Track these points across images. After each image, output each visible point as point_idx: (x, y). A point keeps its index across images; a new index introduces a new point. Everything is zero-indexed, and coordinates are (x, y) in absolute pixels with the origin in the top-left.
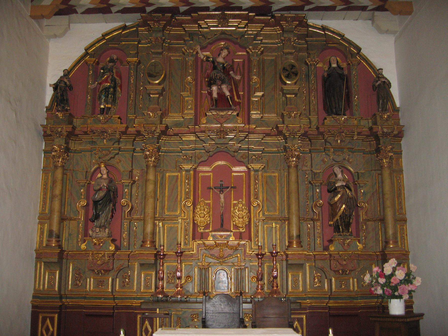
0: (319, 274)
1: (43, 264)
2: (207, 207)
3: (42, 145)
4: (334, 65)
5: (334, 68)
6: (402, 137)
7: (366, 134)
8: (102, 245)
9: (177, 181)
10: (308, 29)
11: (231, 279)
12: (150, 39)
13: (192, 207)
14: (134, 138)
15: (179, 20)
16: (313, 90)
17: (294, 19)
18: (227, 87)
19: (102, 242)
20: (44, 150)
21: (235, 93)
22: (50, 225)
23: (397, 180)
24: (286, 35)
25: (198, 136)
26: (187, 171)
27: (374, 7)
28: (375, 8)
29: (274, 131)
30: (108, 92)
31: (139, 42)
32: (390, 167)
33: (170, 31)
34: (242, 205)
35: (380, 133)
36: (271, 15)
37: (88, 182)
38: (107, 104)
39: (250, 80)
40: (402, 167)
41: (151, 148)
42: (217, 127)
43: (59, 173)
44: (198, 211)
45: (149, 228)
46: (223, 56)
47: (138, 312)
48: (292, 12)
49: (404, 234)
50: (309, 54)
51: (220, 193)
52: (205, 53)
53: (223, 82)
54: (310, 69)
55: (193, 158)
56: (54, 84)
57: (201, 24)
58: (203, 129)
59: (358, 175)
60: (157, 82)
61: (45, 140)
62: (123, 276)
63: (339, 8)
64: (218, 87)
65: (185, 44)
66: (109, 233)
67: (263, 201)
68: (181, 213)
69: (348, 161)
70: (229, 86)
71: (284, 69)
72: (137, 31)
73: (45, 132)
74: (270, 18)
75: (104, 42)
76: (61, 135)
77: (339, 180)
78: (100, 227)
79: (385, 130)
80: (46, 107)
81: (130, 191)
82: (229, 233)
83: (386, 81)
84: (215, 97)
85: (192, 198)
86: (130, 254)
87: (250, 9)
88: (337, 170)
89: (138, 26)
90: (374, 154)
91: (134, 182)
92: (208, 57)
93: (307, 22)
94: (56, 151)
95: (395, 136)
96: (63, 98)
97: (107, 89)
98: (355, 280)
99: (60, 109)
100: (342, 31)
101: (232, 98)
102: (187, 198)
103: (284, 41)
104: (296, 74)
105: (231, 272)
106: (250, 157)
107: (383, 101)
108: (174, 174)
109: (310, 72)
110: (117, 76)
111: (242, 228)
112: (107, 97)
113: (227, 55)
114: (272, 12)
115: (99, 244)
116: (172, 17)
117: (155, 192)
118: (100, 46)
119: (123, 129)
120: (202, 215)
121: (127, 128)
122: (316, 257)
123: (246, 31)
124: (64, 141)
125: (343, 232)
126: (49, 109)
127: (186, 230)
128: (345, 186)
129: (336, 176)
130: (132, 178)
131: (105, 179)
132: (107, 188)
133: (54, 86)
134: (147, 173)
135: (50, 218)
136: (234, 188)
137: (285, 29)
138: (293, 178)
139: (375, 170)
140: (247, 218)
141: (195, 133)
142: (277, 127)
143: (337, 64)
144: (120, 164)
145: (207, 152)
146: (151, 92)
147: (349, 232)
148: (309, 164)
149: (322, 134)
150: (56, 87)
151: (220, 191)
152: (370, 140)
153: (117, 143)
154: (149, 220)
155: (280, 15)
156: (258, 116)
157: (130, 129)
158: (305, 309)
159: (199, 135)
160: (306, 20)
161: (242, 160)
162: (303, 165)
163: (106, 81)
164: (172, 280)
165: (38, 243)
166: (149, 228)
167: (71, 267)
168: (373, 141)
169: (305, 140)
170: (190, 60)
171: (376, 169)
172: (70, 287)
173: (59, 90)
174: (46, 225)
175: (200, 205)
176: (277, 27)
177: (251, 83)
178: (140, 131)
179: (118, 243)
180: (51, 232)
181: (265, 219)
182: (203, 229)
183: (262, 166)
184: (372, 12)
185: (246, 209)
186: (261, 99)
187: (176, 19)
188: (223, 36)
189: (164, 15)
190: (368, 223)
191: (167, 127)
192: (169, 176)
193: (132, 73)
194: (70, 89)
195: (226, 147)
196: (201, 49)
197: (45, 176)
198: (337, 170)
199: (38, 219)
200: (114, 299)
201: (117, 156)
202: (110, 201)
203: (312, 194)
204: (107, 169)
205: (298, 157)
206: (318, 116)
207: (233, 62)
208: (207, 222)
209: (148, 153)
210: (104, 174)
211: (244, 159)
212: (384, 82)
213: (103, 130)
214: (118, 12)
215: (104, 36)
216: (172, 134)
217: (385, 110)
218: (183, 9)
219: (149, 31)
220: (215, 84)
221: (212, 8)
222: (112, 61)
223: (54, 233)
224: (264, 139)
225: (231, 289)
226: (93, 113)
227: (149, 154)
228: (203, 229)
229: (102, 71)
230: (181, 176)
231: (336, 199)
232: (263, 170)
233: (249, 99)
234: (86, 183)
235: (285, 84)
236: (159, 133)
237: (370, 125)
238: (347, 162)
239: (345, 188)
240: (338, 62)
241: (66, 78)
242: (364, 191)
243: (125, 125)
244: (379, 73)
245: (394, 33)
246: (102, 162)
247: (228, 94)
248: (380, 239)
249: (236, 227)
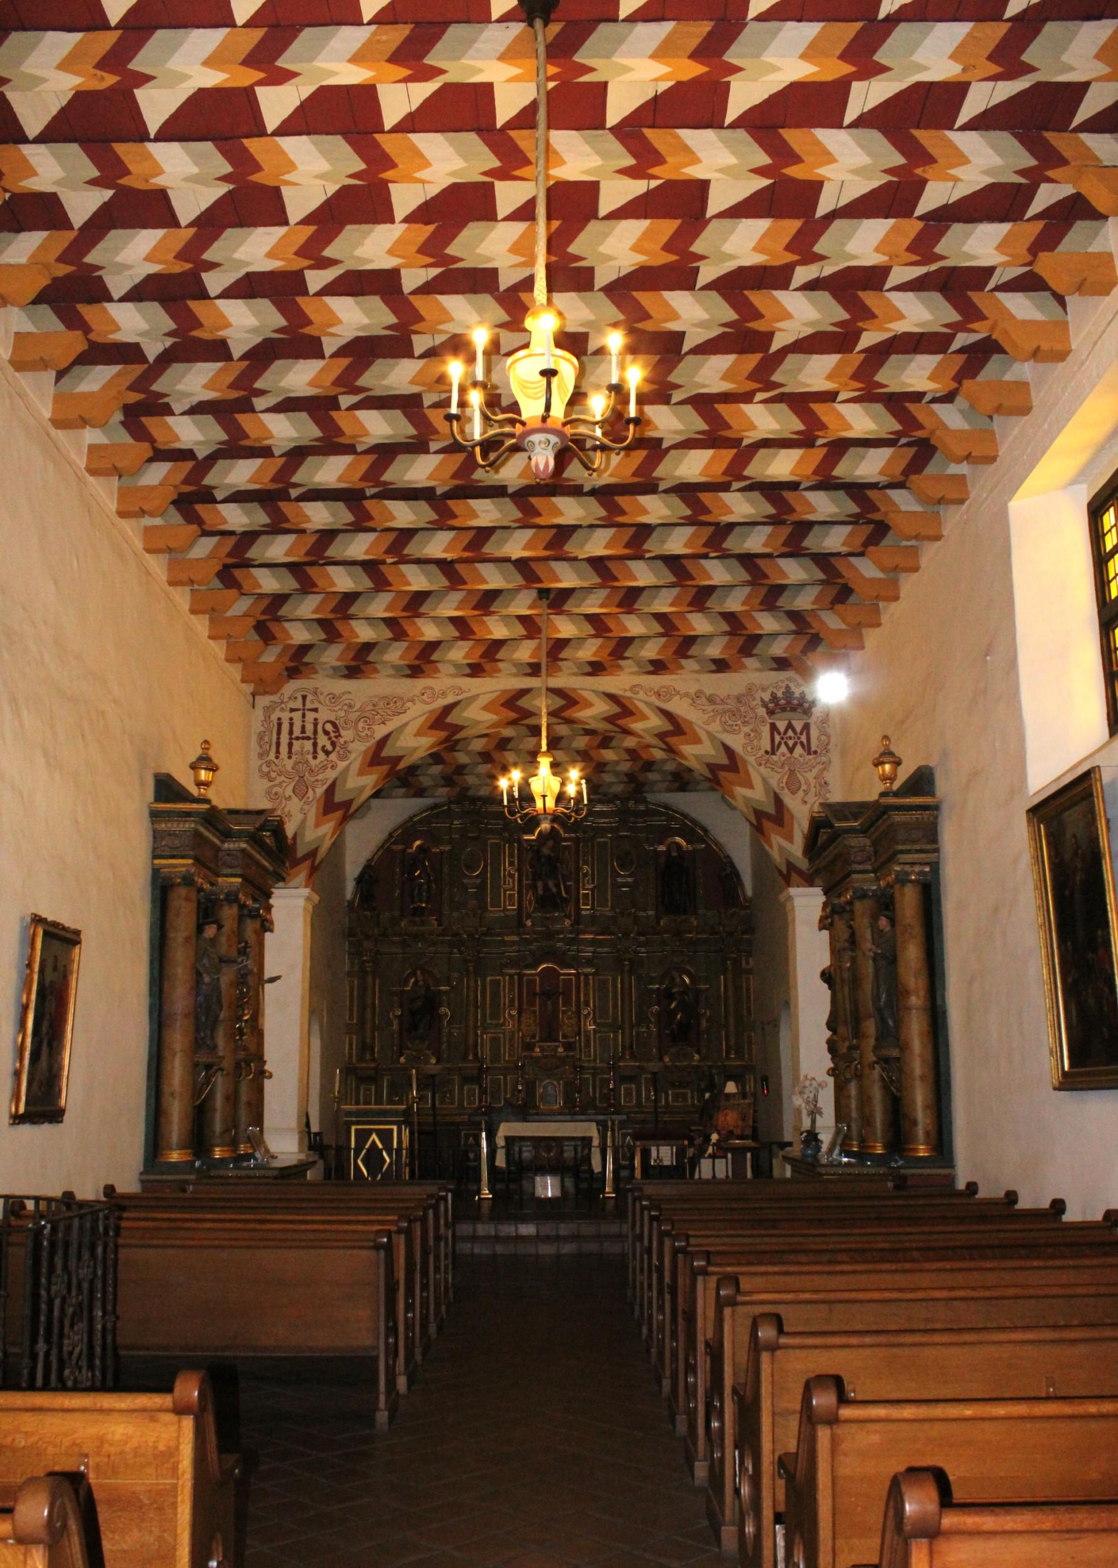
4: (675, 854)
26: (511, 976)
72: (449, 809)
88: (675, 974)
89: (450, 802)
101: (560, 893)
102: (511, 1005)
126: (351, 903)
127: (510, 1040)
150: (359, 880)
198: (675, 974)
215: (411, 818)
247: (554, 890)
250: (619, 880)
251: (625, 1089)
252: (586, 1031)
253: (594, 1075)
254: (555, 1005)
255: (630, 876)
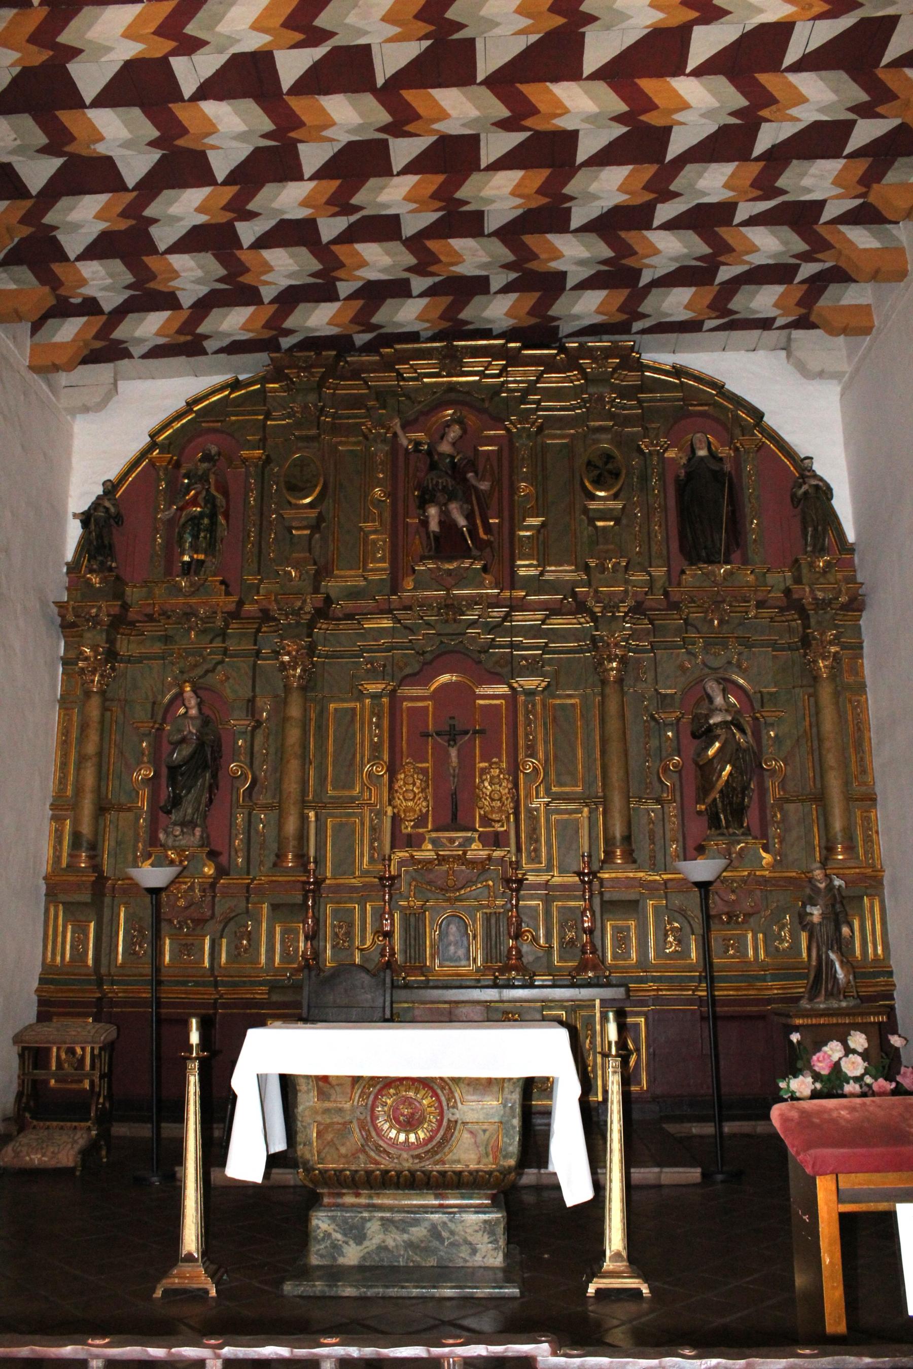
0: (676, 925)
1: (61, 907)
2: (421, 777)
3: (58, 645)
4: (702, 453)
5: (702, 459)
6: (861, 610)
7: (779, 604)
8: (186, 863)
9: (353, 721)
10: (643, 374)
11: (475, 937)
12: (291, 408)
13: (386, 777)
14: (256, 626)
15: (353, 363)
16: (656, 509)
17: (608, 353)
18: (461, 507)
19: (187, 857)
20: (62, 658)
21: (478, 522)
22: (76, 822)
23: (854, 708)
24: (592, 390)
25: (396, 617)
26: (375, 697)
27: (790, 319)
28: (793, 321)
29: (569, 602)
30: (198, 527)
31: (268, 416)
32: (833, 678)
33: (335, 389)
34: (498, 771)
35: (808, 600)
36: (557, 345)
37: (157, 726)
38: (197, 552)
39: (513, 490)
40: (863, 678)
41: (293, 648)
42: (439, 596)
43: (94, 709)
44: (400, 787)
45: (291, 826)
46: (450, 440)
47: (268, 1014)
48: (605, 337)
49: (871, 829)
50: (646, 429)
51: (449, 745)
52: (413, 436)
53: (452, 497)
54: (648, 462)
55: (389, 668)
56: (83, 513)
57: (402, 371)
58: (407, 603)
59: (762, 696)
60: (308, 500)
61: (65, 637)
62: (236, 932)
63: (709, 324)
64: (441, 509)
65: (368, 416)
66: (201, 837)
67: (547, 760)
68: (362, 792)
69: (739, 666)
70: (465, 506)
71: (589, 463)
72: (263, 391)
73: (63, 617)
74: (555, 352)
75: (190, 418)
76: (98, 624)
77: (716, 709)
78: (183, 824)
79: (820, 595)
80: (67, 564)
81: (248, 744)
82: (469, 834)
83: (821, 484)
84: (433, 532)
85: (386, 757)
86: (250, 884)
87: (510, 335)
88: (713, 688)
89: (264, 380)
90: (798, 650)
91: (259, 724)
92: (418, 444)
93: (639, 358)
94: (86, 659)
95: (845, 607)
96: (103, 542)
97: (195, 520)
98: (760, 936)
99: (95, 567)
100: (719, 377)
101: (473, 531)
103: (589, 401)
104: (616, 475)
105: (474, 922)
106: (515, 664)
107: (815, 529)
108: (346, 705)
109: (649, 471)
110: (217, 490)
111: (498, 821)
112: (196, 537)
113: (461, 437)
114: (561, 338)
115: (181, 862)
116: (338, 357)
117: (304, 746)
118: (183, 425)
119: (232, 607)
120: (411, 796)
121: (240, 603)
122: (669, 884)
123: (503, 382)
124: (104, 636)
125: (727, 827)
126: (73, 568)
127: (373, 829)
128: (732, 722)
129: (711, 700)
130: (253, 716)
131: (192, 718)
132: (198, 738)
133: (84, 517)
134: (285, 702)
135: (75, 806)
136: (481, 732)
137: (590, 377)
138: (613, 707)
139: (801, 687)
140: (510, 800)
141: (390, 611)
142: (574, 595)
143: (709, 449)
144: (226, 684)
145: (418, 653)
146: (294, 524)
147: (741, 826)
148: (650, 676)
149: (675, 606)
150: (86, 519)
151: (449, 741)
152: (790, 618)
153: (219, 639)
154: (292, 807)
155: (576, 345)
156: (533, 572)
157: (247, 607)
158: (642, 1003)
159: (399, 617)
160: (637, 353)
161: (498, 670)
162: (637, 679)
163: (194, 502)
164: (344, 942)
165: (51, 862)
166: (291, 826)
167: (122, 915)
168: (795, 620)
169: (640, 622)
170: (380, 451)
171: (804, 683)
172: (120, 957)
173: (93, 527)
174: (68, 821)
175: (404, 772)
176: (572, 371)
177: (516, 498)
178: (269, 610)
179: (223, 859)
180: (76, 836)
181: (550, 802)
182: (412, 827)
183: (543, 681)
184: (785, 332)
185: (508, 780)
186: (539, 532)
187: (347, 362)
188: (453, 396)
189: (320, 354)
190: (786, 806)
191: (328, 600)
192: (336, 710)
193: (251, 483)
194: (117, 523)
195: (461, 642)
196: (403, 427)
197: (65, 715)
198: (713, 688)
199: (51, 809)
200: (216, 984)
201: (219, 667)
202: (205, 767)
203: (658, 744)
204: (198, 697)
205: (623, 660)
206: (669, 567)
207: (476, 451)
208: (420, 810)
209: (286, 658)
210: (191, 708)
211: (501, 666)
212: (817, 487)
213: (189, 610)
214: (221, 351)
215: (190, 404)
216: (341, 615)
217: (821, 550)
218: (361, 339)
219: (288, 389)
220: (433, 502)
221: (424, 335)
222: (207, 458)
223: (84, 839)
224: (548, 621)
225: (475, 960)
226: (169, 572)
227: (289, 662)
228: (412, 827)
229: (186, 481)
230: (363, 705)
231: (711, 752)
232: (546, 693)
233: (512, 533)
234: (152, 728)
235: (593, 497)
236: (309, 613)
237: (789, 582)
238: (737, 670)
239: (731, 729)
240: (709, 443)
241: (109, 500)
242: (776, 735)
243: (235, 598)
244: (803, 466)
245: (835, 376)
246: (185, 681)
247: (462, 522)
248: (816, 842)
249: (486, 821)
250: (593, 505)
251: (617, 930)
252: (529, 811)
253: (548, 901)
254: (467, 760)
255: (615, 497)
